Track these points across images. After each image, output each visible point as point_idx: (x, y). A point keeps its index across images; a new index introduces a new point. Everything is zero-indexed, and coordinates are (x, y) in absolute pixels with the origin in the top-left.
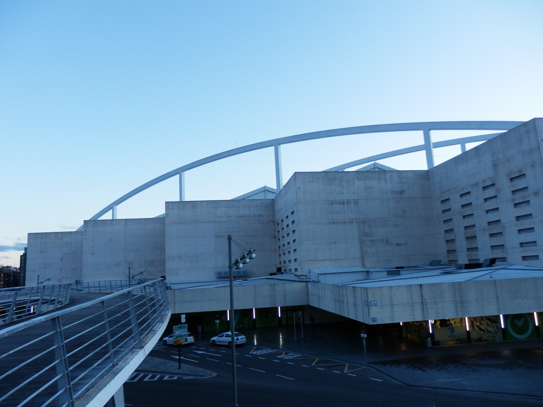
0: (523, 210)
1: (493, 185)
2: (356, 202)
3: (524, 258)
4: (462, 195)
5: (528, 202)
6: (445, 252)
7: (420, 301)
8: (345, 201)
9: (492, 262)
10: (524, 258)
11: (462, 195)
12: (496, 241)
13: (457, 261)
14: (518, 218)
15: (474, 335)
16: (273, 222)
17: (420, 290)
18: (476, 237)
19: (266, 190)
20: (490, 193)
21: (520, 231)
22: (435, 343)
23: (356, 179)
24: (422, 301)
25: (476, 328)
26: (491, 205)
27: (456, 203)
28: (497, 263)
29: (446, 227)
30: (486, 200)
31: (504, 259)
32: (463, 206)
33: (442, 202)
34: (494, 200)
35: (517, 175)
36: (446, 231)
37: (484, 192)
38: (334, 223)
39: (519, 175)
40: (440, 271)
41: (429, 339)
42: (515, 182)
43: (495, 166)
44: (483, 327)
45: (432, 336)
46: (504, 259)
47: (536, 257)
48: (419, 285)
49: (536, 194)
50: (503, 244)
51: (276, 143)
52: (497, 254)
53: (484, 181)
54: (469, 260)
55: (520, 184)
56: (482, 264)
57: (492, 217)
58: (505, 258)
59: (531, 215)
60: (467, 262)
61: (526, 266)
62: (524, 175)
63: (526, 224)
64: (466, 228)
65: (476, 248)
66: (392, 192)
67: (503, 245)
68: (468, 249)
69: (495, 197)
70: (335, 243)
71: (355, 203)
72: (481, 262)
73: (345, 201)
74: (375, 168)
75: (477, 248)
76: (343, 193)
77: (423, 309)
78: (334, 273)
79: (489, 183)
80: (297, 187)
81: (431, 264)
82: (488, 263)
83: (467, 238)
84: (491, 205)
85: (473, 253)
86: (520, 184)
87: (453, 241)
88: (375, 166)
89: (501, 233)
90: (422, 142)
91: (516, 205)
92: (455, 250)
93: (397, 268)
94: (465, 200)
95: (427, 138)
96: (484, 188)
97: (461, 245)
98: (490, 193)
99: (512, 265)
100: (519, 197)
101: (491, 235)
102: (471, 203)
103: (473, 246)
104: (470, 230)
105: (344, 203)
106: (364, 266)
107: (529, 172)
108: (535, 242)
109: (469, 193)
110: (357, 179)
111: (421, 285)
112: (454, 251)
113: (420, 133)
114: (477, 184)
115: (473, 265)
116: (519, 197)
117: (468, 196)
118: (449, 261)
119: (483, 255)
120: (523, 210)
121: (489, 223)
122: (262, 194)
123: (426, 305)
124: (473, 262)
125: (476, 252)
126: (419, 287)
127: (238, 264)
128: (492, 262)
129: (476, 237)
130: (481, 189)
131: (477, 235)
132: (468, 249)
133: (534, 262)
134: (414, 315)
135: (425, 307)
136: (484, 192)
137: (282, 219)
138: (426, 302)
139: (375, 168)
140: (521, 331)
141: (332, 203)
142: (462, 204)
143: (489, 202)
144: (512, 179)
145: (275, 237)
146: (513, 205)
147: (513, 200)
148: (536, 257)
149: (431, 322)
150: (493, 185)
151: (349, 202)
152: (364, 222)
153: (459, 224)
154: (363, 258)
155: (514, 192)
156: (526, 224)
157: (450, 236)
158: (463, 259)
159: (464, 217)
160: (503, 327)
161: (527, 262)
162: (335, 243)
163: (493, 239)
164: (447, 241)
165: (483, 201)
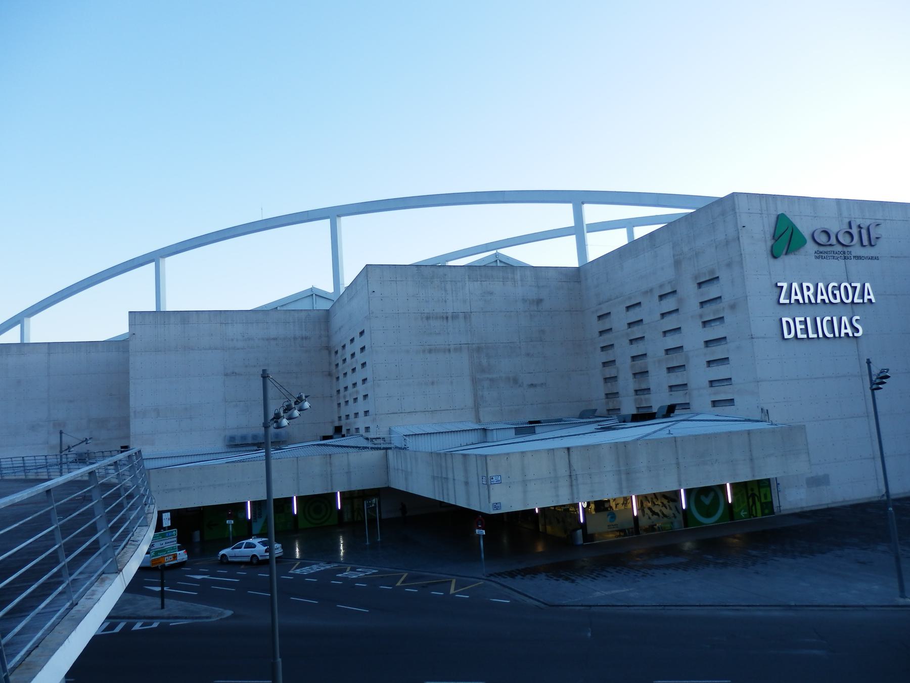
1: (674, 292)
2: (467, 316)
3: (715, 403)
4: (628, 308)
5: (721, 319)
6: (603, 396)
7: (568, 473)
8: (450, 315)
10: (715, 403)
11: (628, 308)
12: (676, 379)
13: (619, 409)
15: (644, 523)
16: (328, 348)
17: (567, 456)
18: (647, 372)
19: (314, 295)
20: (669, 304)
21: (709, 363)
22: (588, 537)
23: (467, 279)
24: (570, 473)
25: (647, 511)
26: (670, 323)
27: (619, 320)
28: (676, 412)
29: (605, 356)
30: (663, 315)
31: (686, 406)
32: (630, 325)
33: (600, 317)
34: (674, 315)
35: (707, 278)
36: (605, 364)
37: (660, 304)
38: (430, 351)
39: (710, 278)
40: (595, 426)
41: (580, 532)
42: (705, 288)
43: (677, 263)
44: (656, 509)
45: (584, 526)
46: (686, 406)
47: (731, 402)
48: (565, 448)
49: (733, 307)
50: (685, 383)
51: (333, 214)
52: (677, 398)
53: (661, 286)
54: (638, 408)
55: (712, 291)
56: (655, 413)
57: (672, 342)
59: (725, 338)
60: (635, 412)
61: (717, 415)
62: (718, 277)
63: (718, 352)
66: (524, 300)
67: (686, 384)
68: (636, 391)
69: (677, 310)
70: (433, 383)
71: (465, 317)
72: (655, 410)
73: (450, 315)
74: (496, 261)
75: (649, 389)
76: (446, 301)
77: (571, 486)
78: (454, 431)
79: (668, 289)
80: (370, 290)
81: (582, 416)
82: (665, 412)
83: (635, 374)
84: (670, 323)
85: (642, 397)
86: (712, 291)
88: (497, 258)
89: (684, 365)
90: (571, 223)
91: (705, 323)
92: (617, 393)
93: (531, 422)
94: (633, 316)
95: (578, 215)
96: (662, 297)
97: (627, 384)
98: (669, 304)
99: (697, 414)
100: (709, 313)
101: (670, 370)
102: (641, 321)
103: (644, 386)
104: (639, 362)
105: (447, 318)
106: (479, 421)
107: (724, 275)
108: (730, 379)
109: (639, 304)
110: (469, 278)
111: (568, 449)
112: (616, 394)
113: (568, 208)
114: (651, 290)
116: (709, 313)
117: (637, 309)
118: (608, 410)
119: (658, 400)
121: (668, 351)
122: (308, 301)
123: (576, 479)
125: (647, 396)
126: (566, 452)
127: (279, 420)
129: (647, 372)
131: (649, 369)
132: (636, 391)
133: (727, 410)
134: (557, 496)
135: (574, 483)
136: (660, 304)
137: (342, 345)
138: (576, 475)
139: (496, 261)
140: (708, 512)
141: (428, 318)
142: (629, 322)
143: (668, 319)
144: (700, 285)
145: (330, 374)
146: (701, 324)
147: (701, 316)
148: (731, 402)
149: (582, 505)
150: (674, 292)
151: (455, 316)
152: (479, 349)
153: (623, 353)
154: (477, 408)
155: (702, 304)
156: (718, 352)
157: (610, 372)
158: (629, 408)
159: (631, 341)
160: (684, 507)
161: (718, 410)
162: (433, 383)
163: (673, 375)
164: (606, 380)
165: (659, 316)
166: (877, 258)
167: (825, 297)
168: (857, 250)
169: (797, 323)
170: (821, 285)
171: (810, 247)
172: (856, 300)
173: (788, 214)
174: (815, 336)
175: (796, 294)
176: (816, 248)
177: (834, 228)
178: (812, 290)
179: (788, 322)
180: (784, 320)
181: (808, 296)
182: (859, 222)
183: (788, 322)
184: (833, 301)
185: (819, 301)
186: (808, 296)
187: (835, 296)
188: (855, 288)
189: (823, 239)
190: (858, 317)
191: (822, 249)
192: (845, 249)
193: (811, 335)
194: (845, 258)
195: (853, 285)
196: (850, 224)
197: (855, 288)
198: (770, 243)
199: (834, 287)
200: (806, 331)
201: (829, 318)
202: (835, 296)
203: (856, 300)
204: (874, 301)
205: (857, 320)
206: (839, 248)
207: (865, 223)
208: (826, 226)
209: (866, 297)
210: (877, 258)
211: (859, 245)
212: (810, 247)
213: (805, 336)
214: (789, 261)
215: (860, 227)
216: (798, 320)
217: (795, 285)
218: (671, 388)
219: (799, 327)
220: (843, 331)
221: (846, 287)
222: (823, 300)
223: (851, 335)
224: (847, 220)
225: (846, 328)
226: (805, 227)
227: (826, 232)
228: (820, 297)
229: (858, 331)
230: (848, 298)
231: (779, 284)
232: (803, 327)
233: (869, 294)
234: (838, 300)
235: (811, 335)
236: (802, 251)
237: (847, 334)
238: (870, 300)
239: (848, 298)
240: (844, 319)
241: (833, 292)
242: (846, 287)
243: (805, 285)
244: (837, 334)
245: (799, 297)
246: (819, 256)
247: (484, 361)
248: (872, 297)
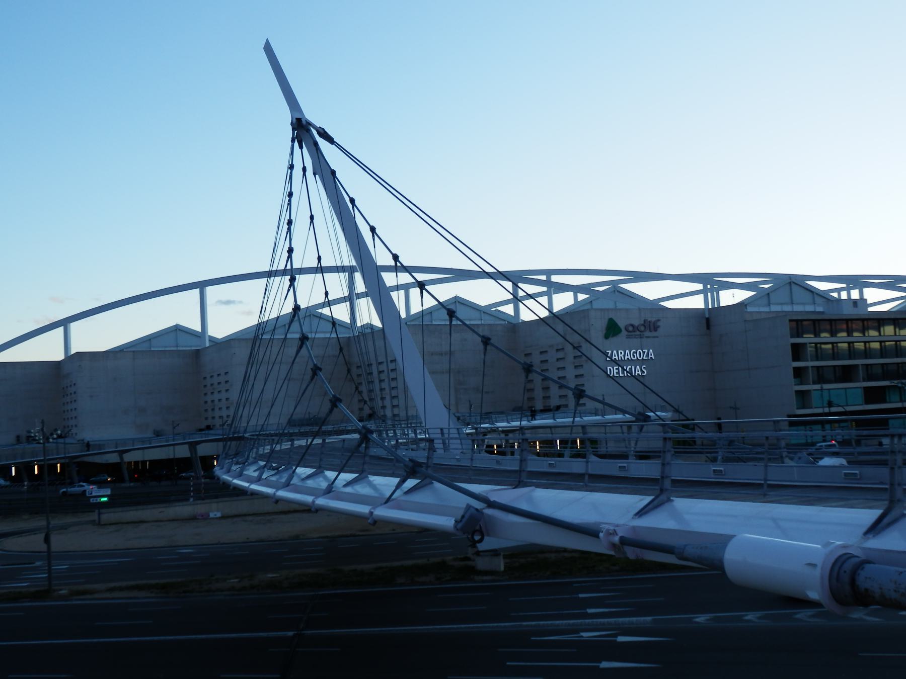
0: (580, 372)
5: (582, 366)
9: (558, 408)
14: (577, 376)
26: (560, 364)
28: (561, 409)
30: (558, 360)
31: (566, 406)
46: (566, 406)
52: (563, 402)
54: (544, 406)
58: (567, 405)
59: (583, 375)
60: (542, 408)
65: (549, 397)
69: (564, 358)
72: (552, 407)
79: (560, 347)
81: (514, 410)
83: (543, 389)
84: (560, 364)
87: (532, 390)
91: (576, 367)
94: (543, 357)
96: (557, 350)
97: (539, 393)
103: (547, 395)
115: (546, 410)
119: (554, 402)
120: (580, 372)
124: (547, 408)
128: (558, 408)
132: (544, 398)
141: (432, 354)
146: (573, 367)
158: (539, 406)
166: (657, 337)
167: (629, 357)
168: (647, 333)
169: (615, 369)
170: (627, 351)
171: (624, 333)
172: (644, 358)
173: (615, 319)
174: (623, 375)
175: (615, 356)
176: (626, 333)
178: (623, 353)
179: (610, 369)
180: (608, 368)
181: (621, 357)
182: (649, 320)
183: (610, 369)
184: (633, 359)
185: (626, 359)
186: (621, 357)
187: (634, 356)
188: (645, 352)
189: (631, 329)
190: (644, 366)
191: (630, 334)
192: (642, 333)
193: (621, 375)
194: (641, 338)
195: (644, 351)
196: (645, 321)
197: (645, 352)
198: (604, 332)
199: (634, 352)
200: (618, 373)
201: (630, 367)
202: (634, 356)
203: (644, 358)
204: (653, 358)
205: (644, 368)
206: (638, 333)
207: (653, 320)
208: (633, 322)
209: (650, 356)
210: (657, 337)
211: (648, 331)
212: (624, 333)
213: (618, 375)
214: (613, 340)
215: (650, 322)
216: (615, 368)
217: (615, 352)
218: (560, 397)
219: (615, 371)
220: (637, 373)
221: (640, 352)
222: (628, 359)
223: (640, 374)
224: (643, 319)
225: (638, 371)
226: (622, 324)
227: (632, 325)
228: (626, 357)
229: (644, 372)
230: (640, 357)
231: (607, 351)
232: (617, 371)
233: (651, 355)
234: (636, 358)
235: (621, 375)
236: (620, 335)
237: (638, 374)
238: (651, 358)
239: (640, 357)
240: (638, 367)
241: (633, 354)
242: (640, 352)
243: (619, 351)
244: (633, 374)
245: (617, 357)
246: (628, 337)
248: (653, 356)
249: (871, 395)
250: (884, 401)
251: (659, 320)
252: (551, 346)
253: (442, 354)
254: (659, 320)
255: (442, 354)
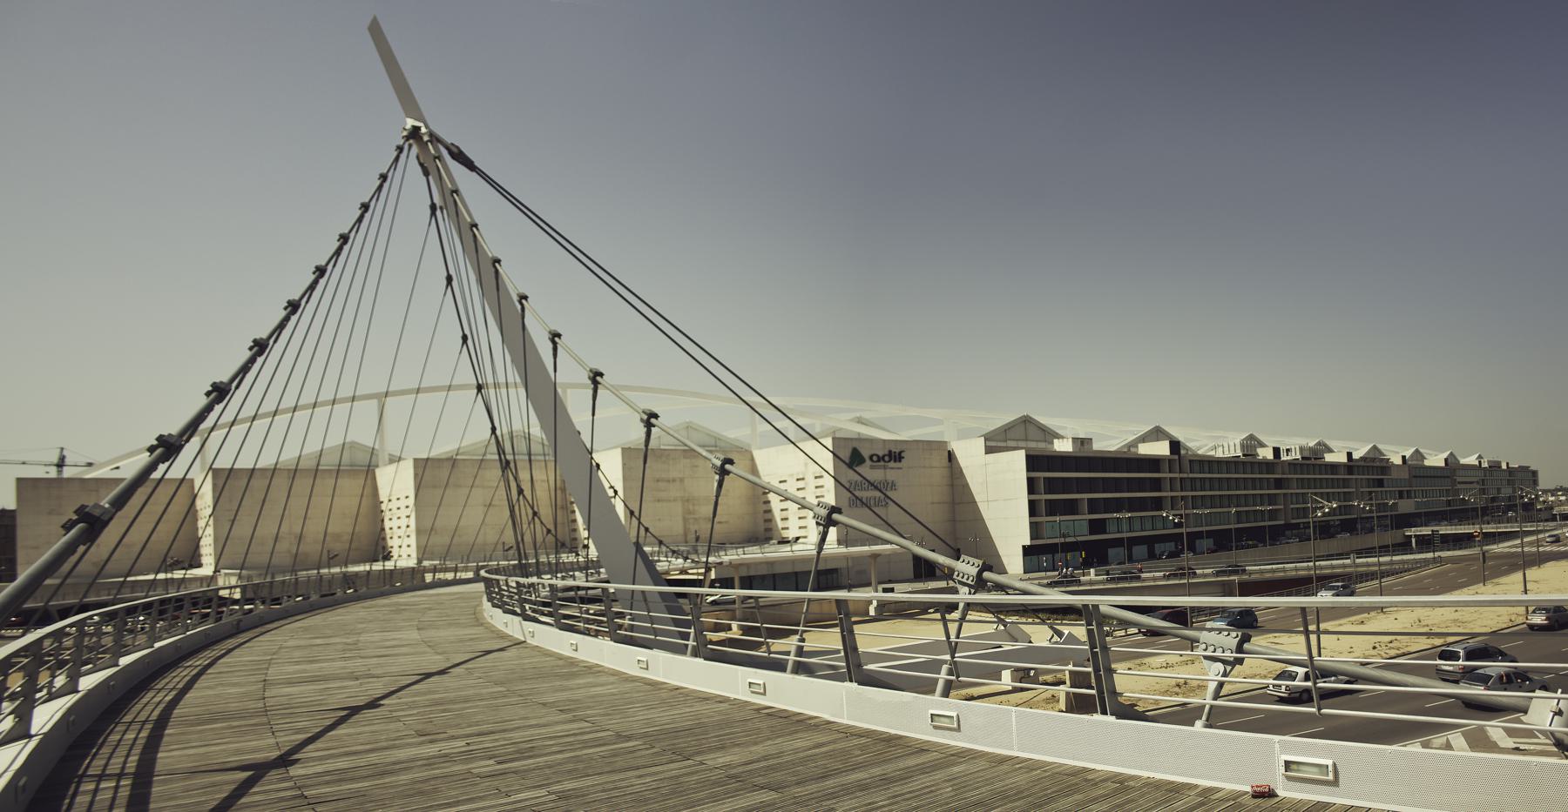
20: (801, 484)
64: (782, 510)
72: (790, 539)
79: (801, 477)
98: (801, 484)
103: (786, 526)
117: (784, 484)
130: (795, 480)
131: (789, 517)
147: (815, 493)
151: (674, 480)
152: (688, 500)
155: (817, 487)
166: (901, 468)
168: (892, 464)
171: (868, 462)
173: (860, 450)
177: (881, 454)
182: (893, 450)
196: (890, 451)
207: (897, 451)
210: (901, 468)
212: (868, 462)
218: (800, 528)
226: (866, 453)
236: (863, 465)
247: (691, 507)
249: (1097, 527)
250: (1105, 532)
251: (903, 451)
252: (792, 475)
253: (669, 481)
254: (903, 451)
255: (669, 481)
